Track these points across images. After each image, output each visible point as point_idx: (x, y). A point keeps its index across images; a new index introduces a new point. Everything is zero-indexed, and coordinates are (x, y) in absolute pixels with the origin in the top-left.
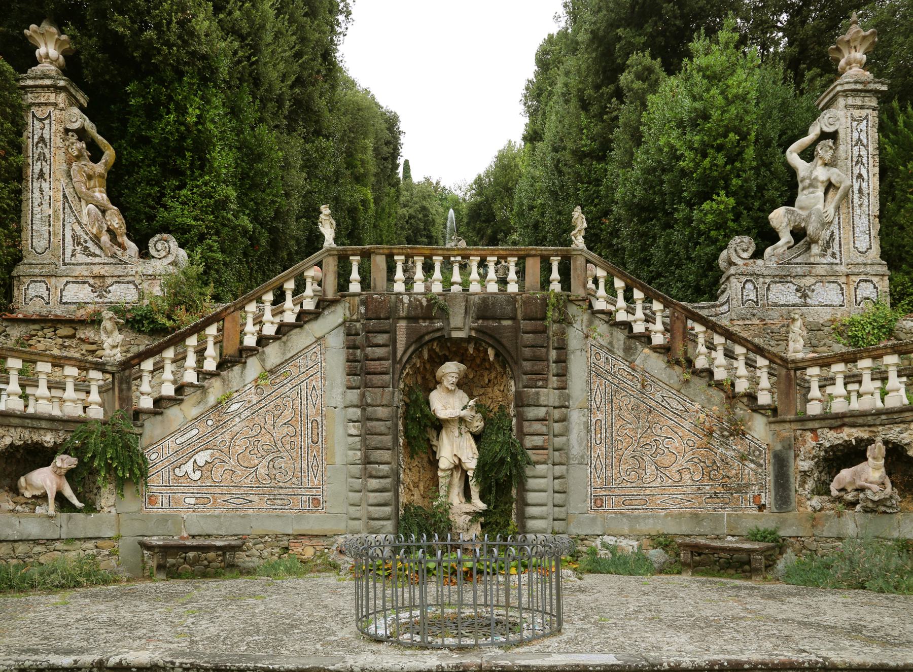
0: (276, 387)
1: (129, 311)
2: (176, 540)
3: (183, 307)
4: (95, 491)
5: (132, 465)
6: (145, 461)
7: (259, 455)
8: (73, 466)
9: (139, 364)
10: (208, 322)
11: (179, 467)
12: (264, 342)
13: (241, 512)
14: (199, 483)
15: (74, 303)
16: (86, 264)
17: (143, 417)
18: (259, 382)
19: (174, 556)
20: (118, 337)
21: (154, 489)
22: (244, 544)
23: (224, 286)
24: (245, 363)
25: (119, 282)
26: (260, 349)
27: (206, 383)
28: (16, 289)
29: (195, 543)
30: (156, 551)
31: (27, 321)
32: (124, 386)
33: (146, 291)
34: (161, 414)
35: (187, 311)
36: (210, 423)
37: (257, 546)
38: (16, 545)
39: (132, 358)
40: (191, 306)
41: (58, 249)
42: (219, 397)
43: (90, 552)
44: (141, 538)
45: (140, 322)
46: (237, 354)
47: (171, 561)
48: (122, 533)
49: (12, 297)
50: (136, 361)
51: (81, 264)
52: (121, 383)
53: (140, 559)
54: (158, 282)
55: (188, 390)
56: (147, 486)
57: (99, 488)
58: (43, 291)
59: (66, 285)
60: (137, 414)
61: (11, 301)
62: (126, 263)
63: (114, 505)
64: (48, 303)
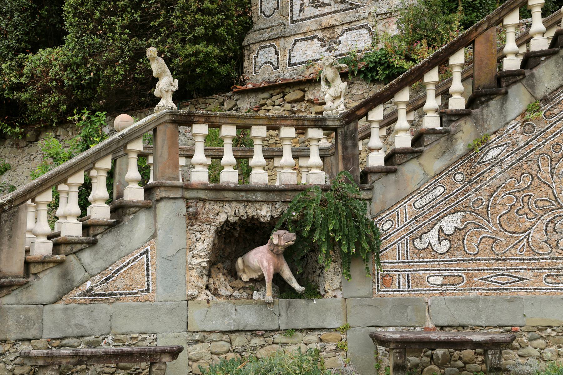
0: (553, 120)
1: (362, 60)
2: (418, 333)
3: (424, 42)
4: (319, 271)
5: (360, 238)
6: (376, 232)
7: (531, 215)
8: (291, 243)
9: (366, 114)
10: (453, 49)
11: (420, 237)
12: (532, 61)
13: (507, 294)
14: (447, 257)
15: (303, 63)
16: (315, 17)
17: (372, 178)
18: (527, 116)
19: (417, 353)
20: (341, 86)
21: (389, 267)
22: (514, 338)
23: (478, 10)
24: (506, 93)
25: (350, 30)
26: (527, 72)
27: (452, 128)
28: (246, 58)
29: (443, 336)
30: (392, 346)
31: (257, 90)
32: (349, 143)
33: (381, 33)
34: (395, 171)
35: (429, 45)
36: (459, 177)
37: (535, 343)
38: (233, 336)
39: (358, 108)
40: (434, 39)
41: (286, 7)
42: (471, 142)
43: (313, 346)
44: (373, 329)
45: (374, 69)
46: (495, 84)
47: (413, 360)
48: (350, 323)
49: (242, 67)
50: (363, 111)
51: (309, 18)
52: (345, 139)
53: (374, 356)
54: (395, 20)
55: (428, 139)
56: (379, 263)
57: (322, 268)
58: (272, 57)
59: (294, 44)
60: (365, 175)
61: (242, 73)
62: (358, 6)
63: (340, 288)
64: (277, 68)
